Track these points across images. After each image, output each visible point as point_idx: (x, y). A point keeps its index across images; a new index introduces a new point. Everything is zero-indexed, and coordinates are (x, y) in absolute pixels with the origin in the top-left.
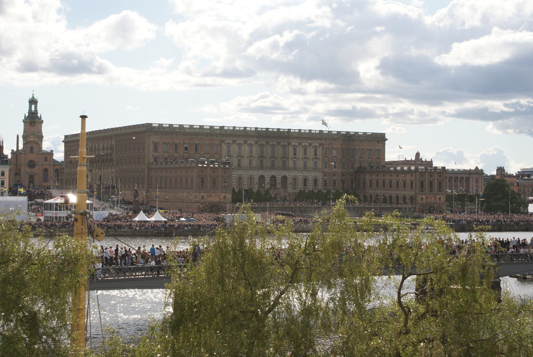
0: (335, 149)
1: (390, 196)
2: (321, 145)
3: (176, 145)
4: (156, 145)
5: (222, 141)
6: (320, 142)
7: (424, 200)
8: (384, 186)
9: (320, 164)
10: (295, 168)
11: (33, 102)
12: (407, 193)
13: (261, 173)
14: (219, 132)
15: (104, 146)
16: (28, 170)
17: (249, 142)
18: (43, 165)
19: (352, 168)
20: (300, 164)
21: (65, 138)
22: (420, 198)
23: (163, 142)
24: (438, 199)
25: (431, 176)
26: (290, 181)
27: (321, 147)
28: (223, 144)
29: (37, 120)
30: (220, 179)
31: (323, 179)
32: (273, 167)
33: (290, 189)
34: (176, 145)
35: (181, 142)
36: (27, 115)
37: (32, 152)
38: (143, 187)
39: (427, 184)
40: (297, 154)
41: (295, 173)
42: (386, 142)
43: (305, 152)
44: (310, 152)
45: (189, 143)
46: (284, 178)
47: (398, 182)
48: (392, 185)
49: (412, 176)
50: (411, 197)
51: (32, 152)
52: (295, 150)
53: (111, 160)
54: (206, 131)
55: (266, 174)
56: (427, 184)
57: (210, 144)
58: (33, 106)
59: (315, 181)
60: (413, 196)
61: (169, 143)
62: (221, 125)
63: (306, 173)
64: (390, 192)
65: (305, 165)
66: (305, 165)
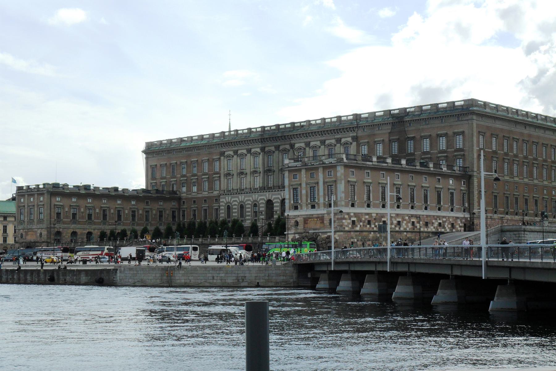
6: (352, 134)
7: (301, 228)
13: (267, 196)
22: (293, 222)
25: (312, 176)
28: (222, 158)
30: (36, 209)
35: (178, 163)
55: (274, 197)
56: (304, 192)
57: (208, 159)
61: (166, 164)
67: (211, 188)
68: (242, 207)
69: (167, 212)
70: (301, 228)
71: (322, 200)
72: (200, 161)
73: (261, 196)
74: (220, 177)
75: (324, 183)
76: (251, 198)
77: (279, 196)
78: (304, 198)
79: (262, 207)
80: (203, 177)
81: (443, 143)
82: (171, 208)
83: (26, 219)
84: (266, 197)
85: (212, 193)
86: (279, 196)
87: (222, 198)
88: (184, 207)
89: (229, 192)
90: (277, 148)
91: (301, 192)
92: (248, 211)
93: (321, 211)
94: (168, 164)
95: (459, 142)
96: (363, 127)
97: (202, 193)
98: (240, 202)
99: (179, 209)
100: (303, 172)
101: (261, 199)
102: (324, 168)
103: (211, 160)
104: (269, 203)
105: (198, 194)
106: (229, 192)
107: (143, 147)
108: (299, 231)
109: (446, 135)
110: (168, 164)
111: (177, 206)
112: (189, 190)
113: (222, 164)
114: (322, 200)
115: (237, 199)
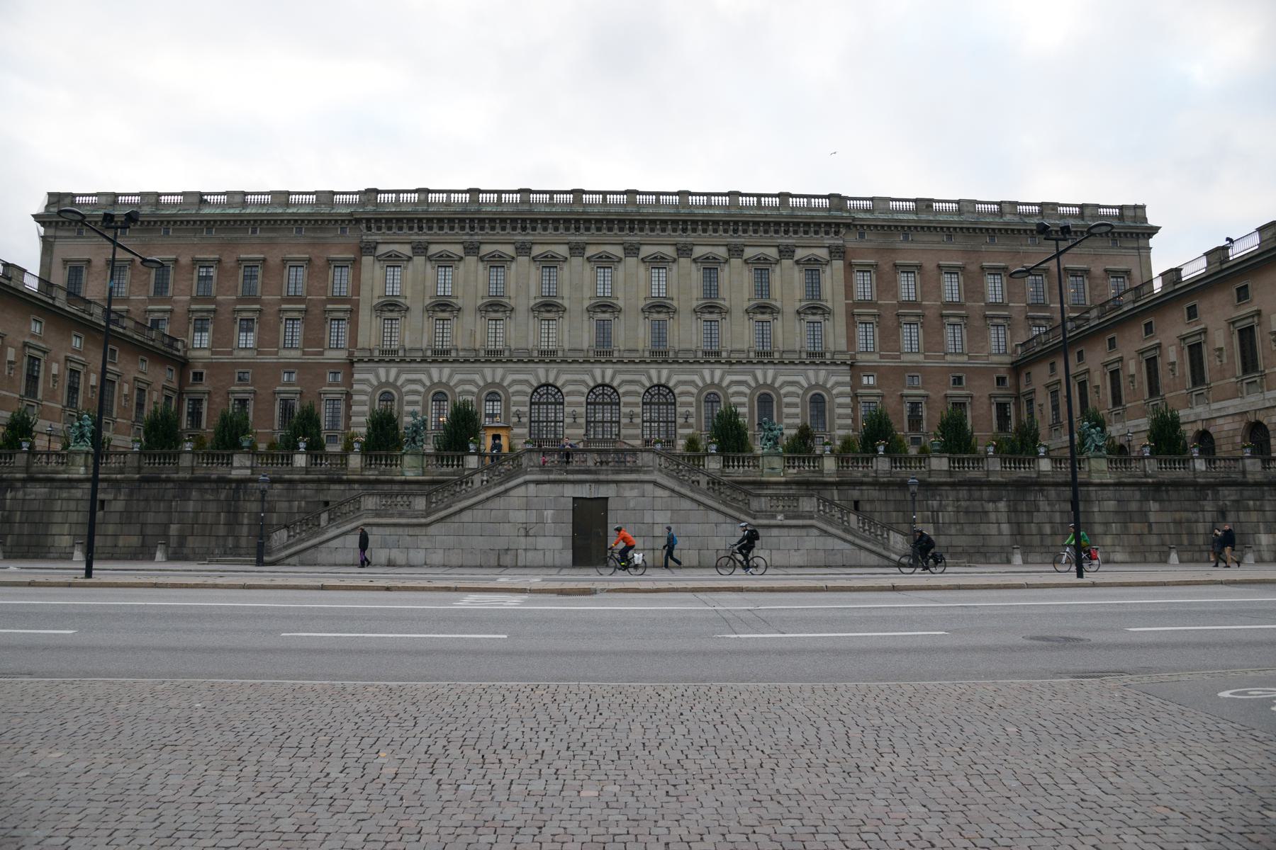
0: (908, 269)
6: (829, 241)
9: (834, 335)
13: (542, 373)
27: (838, 264)
31: (855, 397)
32: (603, 353)
35: (185, 260)
40: (724, 292)
42: (1152, 242)
43: (763, 286)
45: (219, 261)
59: (818, 403)
63: (766, 374)
67: (314, 340)
69: (155, 396)
72: (274, 257)
74: (354, 312)
76: (477, 377)
80: (284, 306)
82: (164, 387)
84: (537, 376)
85: (321, 353)
88: (199, 388)
89: (389, 357)
97: (276, 353)
98: (433, 384)
99: (180, 394)
101: (514, 382)
103: (319, 262)
105: (259, 353)
106: (389, 357)
107: (39, 206)
111: (175, 386)
112: (222, 341)
113: (365, 275)
115: (423, 377)
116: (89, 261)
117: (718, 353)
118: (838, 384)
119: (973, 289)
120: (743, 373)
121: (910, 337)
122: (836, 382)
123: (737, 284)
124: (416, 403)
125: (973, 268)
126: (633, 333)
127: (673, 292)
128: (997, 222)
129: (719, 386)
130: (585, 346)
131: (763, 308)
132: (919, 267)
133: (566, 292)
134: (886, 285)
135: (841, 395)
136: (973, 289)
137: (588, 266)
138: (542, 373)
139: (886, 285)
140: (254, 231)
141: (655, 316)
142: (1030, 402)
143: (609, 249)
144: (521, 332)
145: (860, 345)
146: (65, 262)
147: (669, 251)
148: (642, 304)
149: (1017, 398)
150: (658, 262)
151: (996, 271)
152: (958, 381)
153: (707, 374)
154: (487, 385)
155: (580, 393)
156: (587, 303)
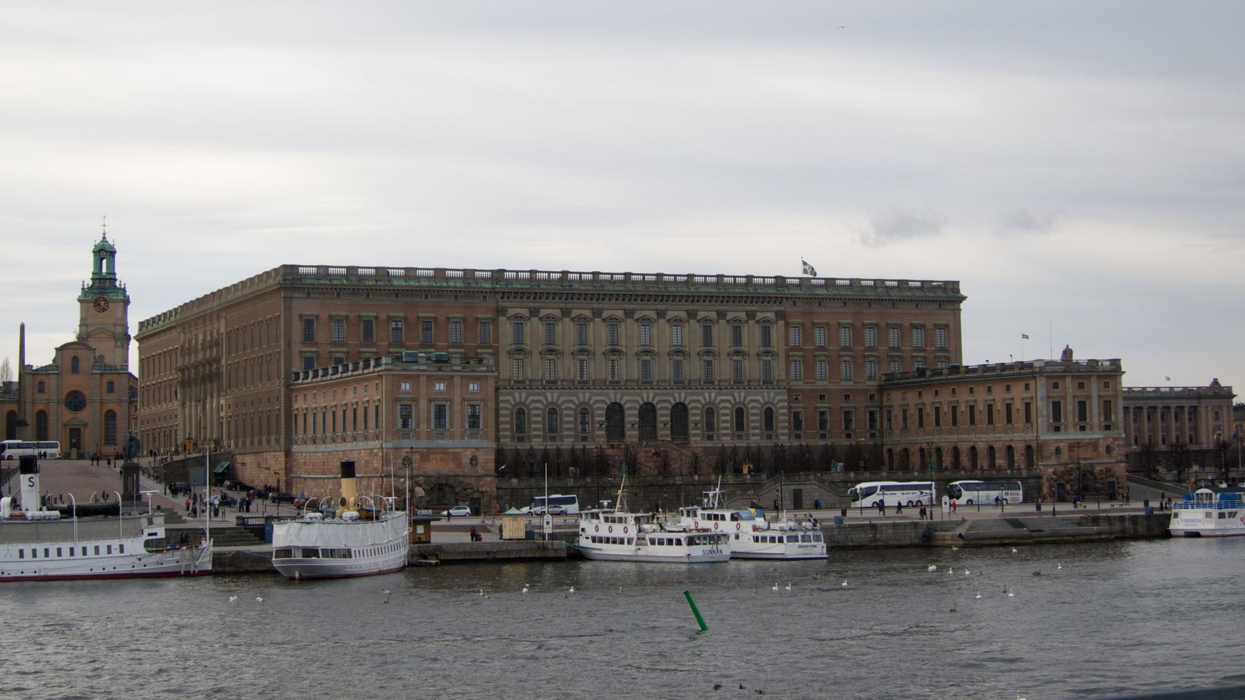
0: (820, 326)
1: (973, 449)
2: (780, 315)
3: (368, 325)
4: (309, 323)
5: (500, 311)
6: (777, 308)
7: (1065, 456)
8: (955, 423)
10: (709, 382)
11: (104, 252)
12: (1017, 436)
14: (488, 285)
15: (204, 340)
16: (68, 415)
17: (575, 313)
18: (102, 403)
19: (870, 378)
20: (724, 369)
21: (140, 330)
22: (1053, 448)
23: (330, 317)
24: (1102, 449)
25: (1081, 386)
26: (695, 416)
27: (781, 323)
28: (502, 319)
29: (113, 296)
31: (790, 408)
32: (646, 382)
33: (697, 439)
34: (368, 325)
35: (383, 316)
36: (91, 283)
37: (75, 369)
38: (277, 441)
39: (1070, 407)
40: (715, 342)
41: (709, 396)
42: (963, 305)
43: (737, 338)
44: (752, 336)
45: (406, 318)
46: (680, 411)
47: (990, 407)
48: (977, 416)
49: (1027, 387)
50: (1029, 447)
51: (75, 369)
52: (707, 332)
53: (218, 375)
54: (452, 284)
55: (625, 398)
56: (1070, 407)
57: (465, 320)
58: (104, 262)
59: (769, 415)
60: (1034, 445)
61: (347, 318)
62: (496, 268)
63: (740, 395)
64: (972, 436)
65: (738, 369)
66: (738, 369)
68: (553, 412)
70: (1065, 456)
71: (1096, 420)
73: (599, 395)
74: (496, 355)
75: (1100, 397)
76: (574, 398)
77: (638, 398)
78: (1070, 416)
79: (599, 415)
81: (893, 337)
83: (423, 427)
86: (638, 398)
87: (504, 394)
89: (520, 384)
90: (629, 314)
91: (1065, 408)
92: (568, 421)
93: (1097, 435)
94: (352, 315)
95: (940, 339)
96: (794, 300)
98: (549, 404)
100: (1068, 380)
101: (597, 401)
102: (1099, 377)
104: (615, 411)
106: (520, 384)
108: (1063, 461)
109: (922, 327)
110: (352, 315)
113: (501, 330)
114: (1096, 420)
116: (317, 317)
117: (712, 383)
118: (780, 401)
119: (858, 338)
120: (727, 394)
121: (821, 369)
122: (779, 400)
123: (722, 336)
124: (538, 415)
125: (859, 324)
126: (663, 369)
127: (686, 343)
128: (871, 294)
129: (713, 403)
130: (636, 377)
131: (738, 353)
132: (827, 325)
133: (623, 342)
134: (808, 336)
135: (782, 408)
136: (858, 338)
137: (636, 325)
138: (612, 396)
139: (808, 336)
140: (427, 297)
141: (676, 358)
142: (889, 412)
143: (647, 313)
144: (598, 369)
145: (792, 376)
146: (301, 316)
147: (683, 315)
148: (668, 349)
149: (881, 408)
150: (677, 321)
151: (871, 326)
152: (847, 397)
153: (707, 395)
154: (580, 404)
155: (634, 408)
156: (636, 350)
